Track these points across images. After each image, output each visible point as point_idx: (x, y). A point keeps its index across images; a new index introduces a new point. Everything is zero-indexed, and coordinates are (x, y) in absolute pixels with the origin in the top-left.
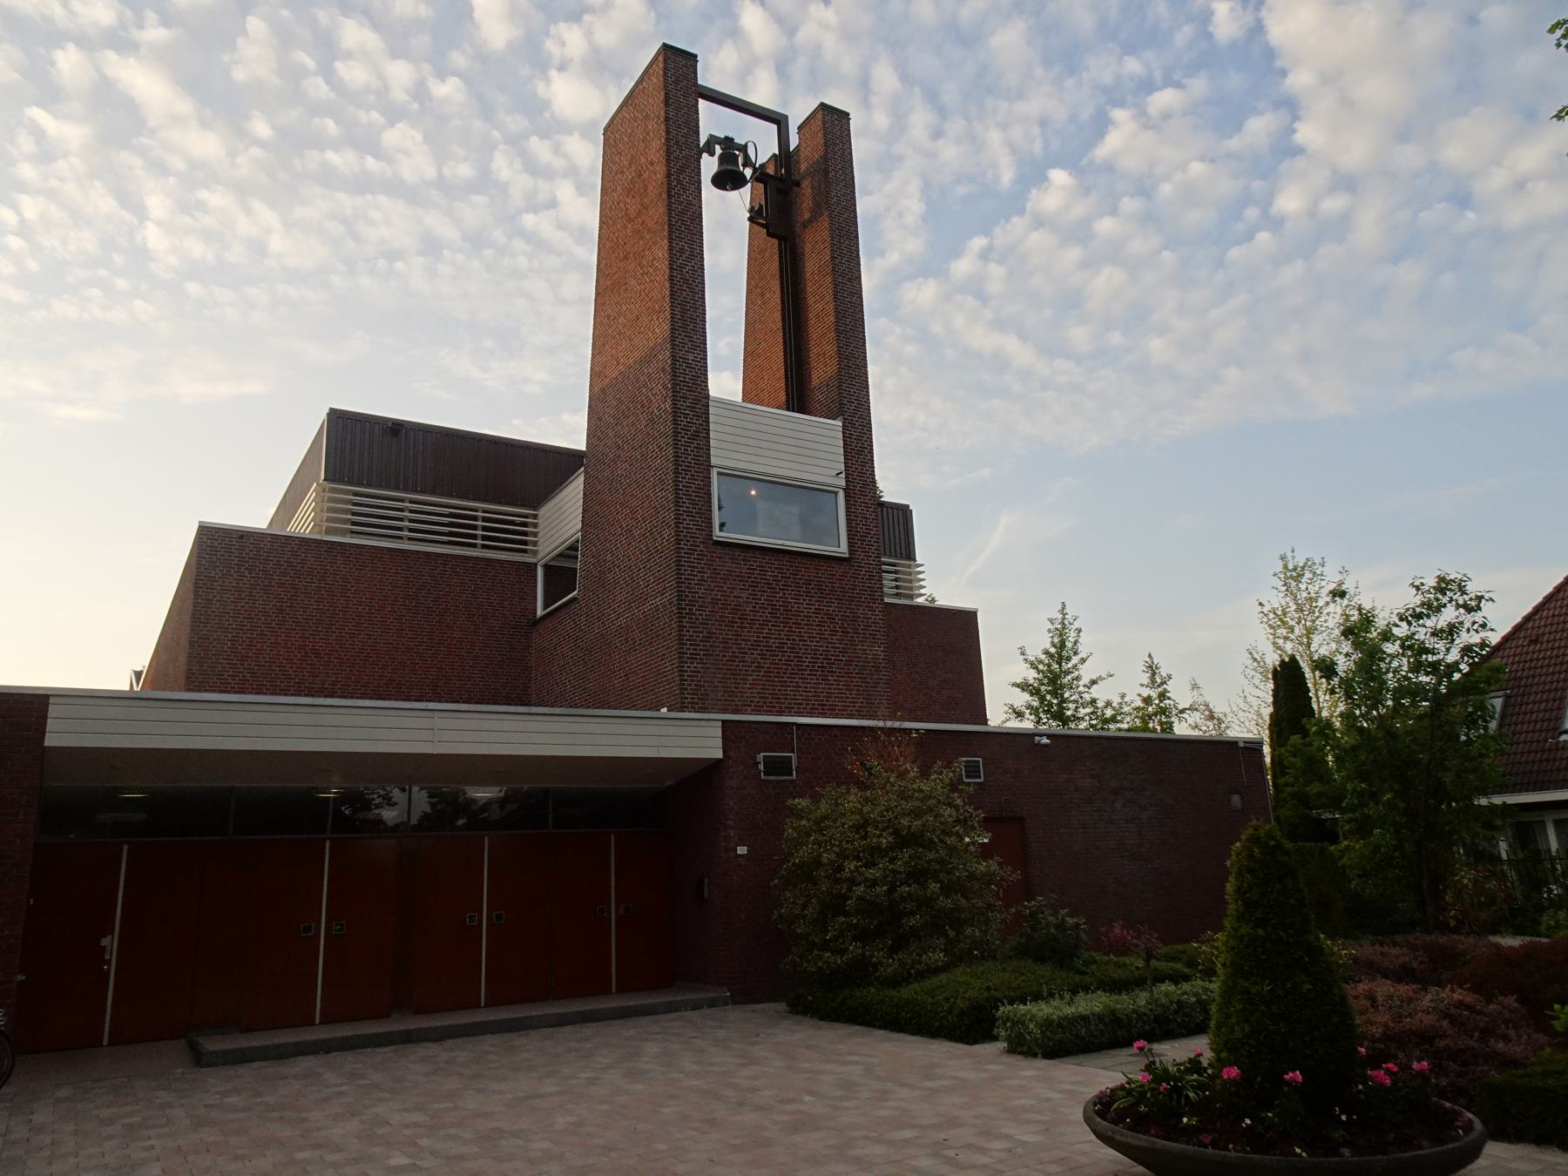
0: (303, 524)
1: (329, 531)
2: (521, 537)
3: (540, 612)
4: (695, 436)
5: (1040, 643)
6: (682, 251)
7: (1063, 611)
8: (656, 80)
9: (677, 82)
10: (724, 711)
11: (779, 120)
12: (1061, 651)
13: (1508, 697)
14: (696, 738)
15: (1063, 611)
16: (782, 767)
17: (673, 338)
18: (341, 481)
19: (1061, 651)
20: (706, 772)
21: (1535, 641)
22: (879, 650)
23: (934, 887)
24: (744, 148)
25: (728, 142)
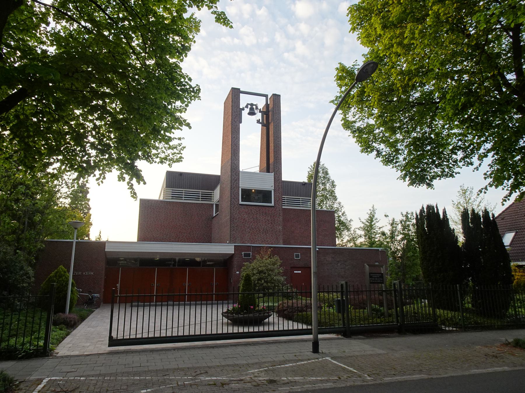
0: (161, 199)
1: (166, 199)
2: (209, 197)
3: (214, 215)
4: (236, 180)
5: (365, 217)
6: (234, 137)
7: (373, 207)
8: (231, 96)
9: (235, 96)
10: (235, 243)
11: (266, 96)
12: (371, 219)
13: (517, 232)
14: (228, 249)
15: (373, 207)
16: (249, 255)
17: (231, 158)
18: (169, 187)
19: (371, 219)
20: (232, 256)
21: (502, 219)
22: (280, 227)
23: (263, 281)
24: (256, 105)
25: (252, 105)
